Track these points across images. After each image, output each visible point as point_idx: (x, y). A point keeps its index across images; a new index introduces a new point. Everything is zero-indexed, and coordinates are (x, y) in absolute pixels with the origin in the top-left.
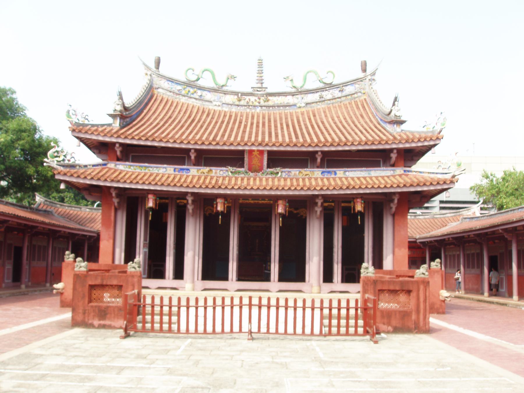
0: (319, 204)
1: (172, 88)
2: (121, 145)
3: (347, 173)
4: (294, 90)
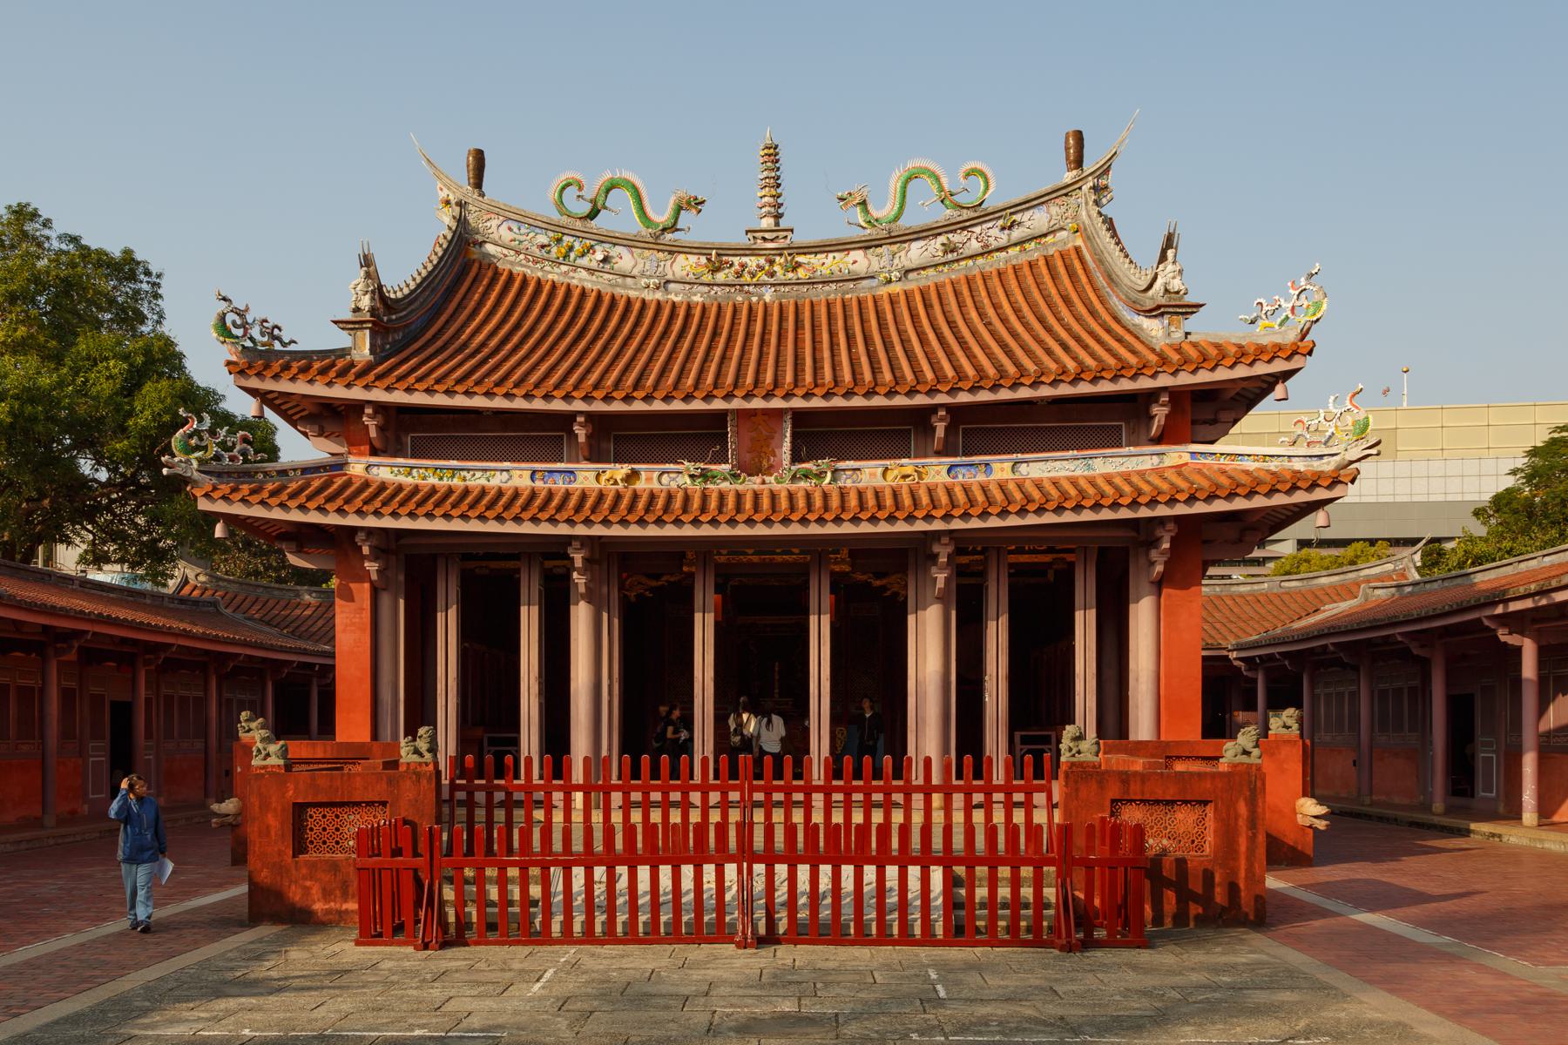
0: (943, 559)
1: (521, 242)
2: (380, 408)
3: (1023, 468)
4: (869, 232)
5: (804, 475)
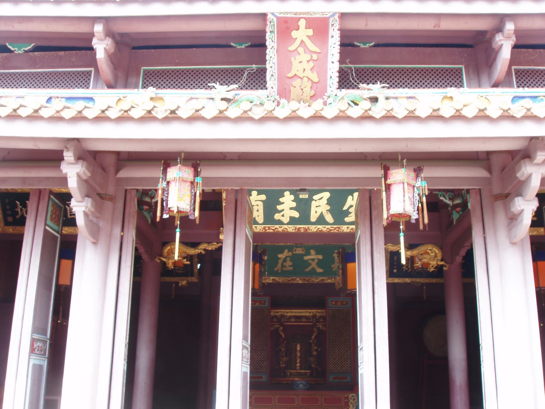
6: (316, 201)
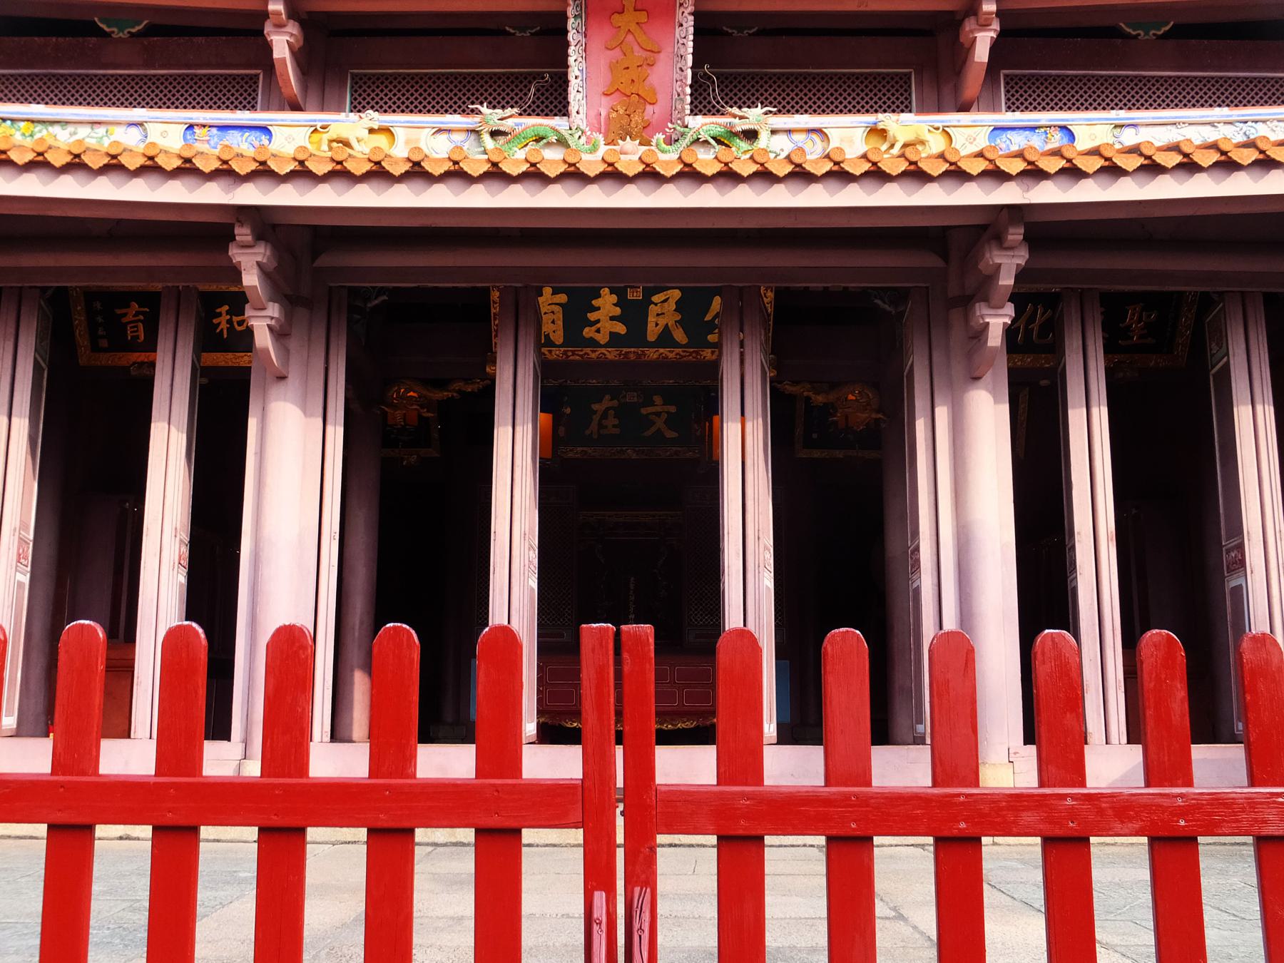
0: (1007, 280)
5: (714, 138)
6: (656, 304)
